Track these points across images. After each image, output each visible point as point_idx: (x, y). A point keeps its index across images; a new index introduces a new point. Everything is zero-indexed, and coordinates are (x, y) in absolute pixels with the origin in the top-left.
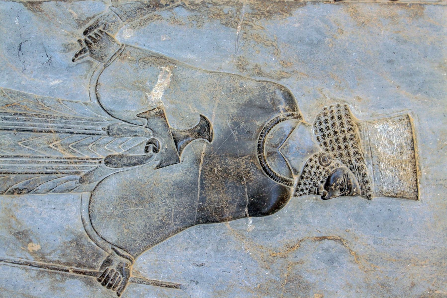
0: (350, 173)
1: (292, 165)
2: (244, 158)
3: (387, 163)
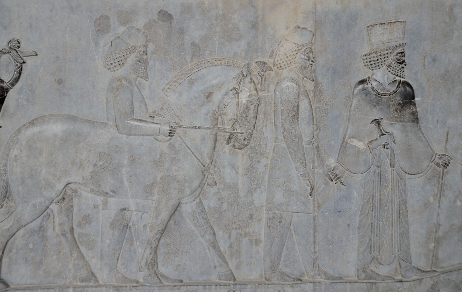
2: (390, 102)
3: (391, 36)
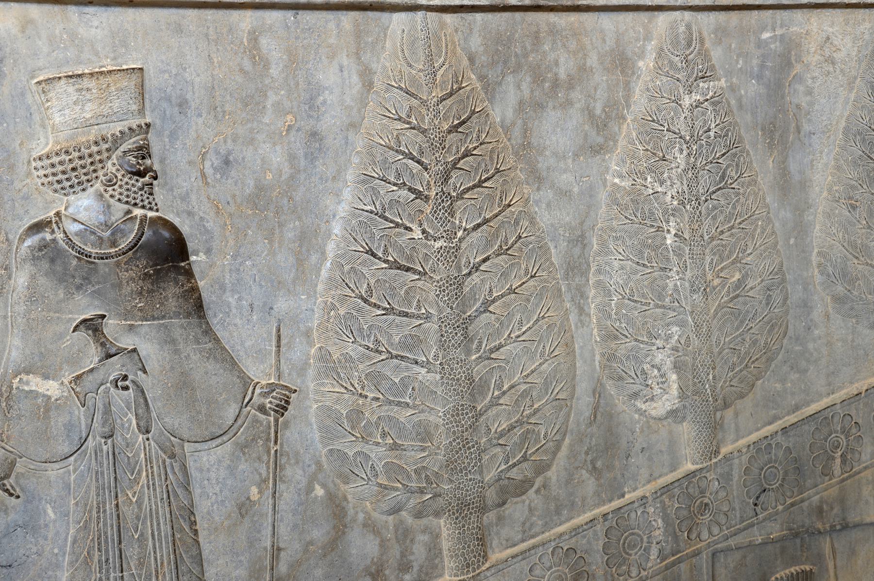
0: (122, 149)
1: (121, 216)
3: (103, 107)
